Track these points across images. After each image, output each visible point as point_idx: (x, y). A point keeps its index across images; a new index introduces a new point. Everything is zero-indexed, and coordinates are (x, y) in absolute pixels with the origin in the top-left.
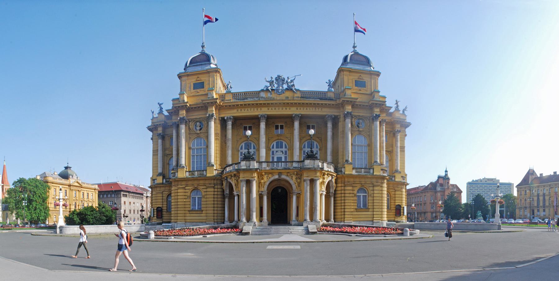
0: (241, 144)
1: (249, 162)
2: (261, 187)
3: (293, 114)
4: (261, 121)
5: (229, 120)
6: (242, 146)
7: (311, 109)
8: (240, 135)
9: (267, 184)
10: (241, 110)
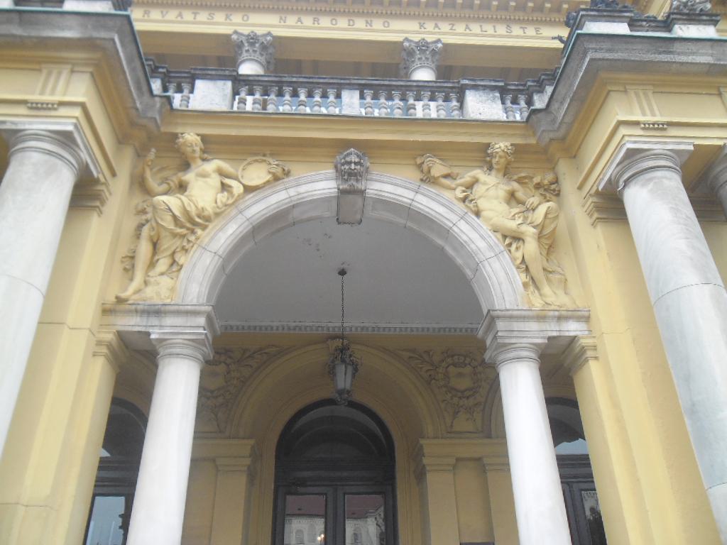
2: (152, 264)
9: (224, 236)
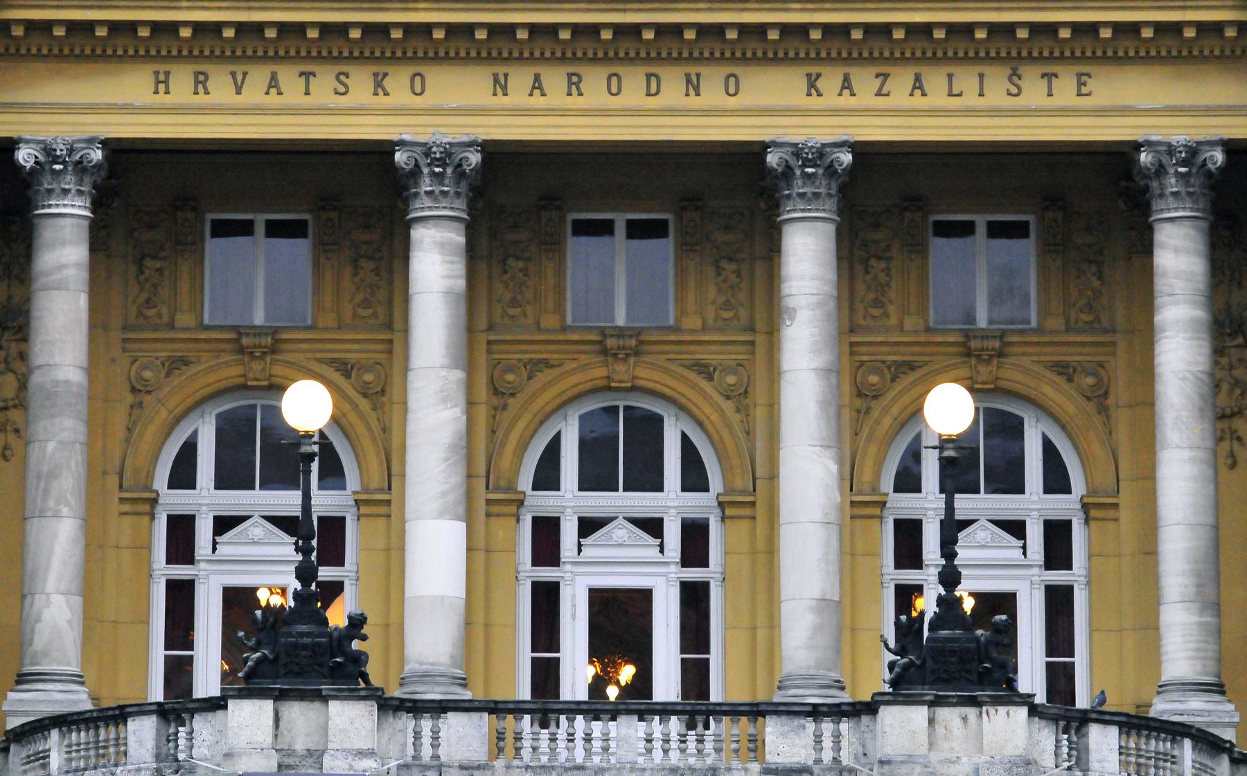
0: (178, 420)
1: (317, 705)
3: (763, 147)
4: (421, 207)
5: (69, 182)
6: (188, 453)
7: (966, 79)
8: (171, 326)
10: (201, 81)
